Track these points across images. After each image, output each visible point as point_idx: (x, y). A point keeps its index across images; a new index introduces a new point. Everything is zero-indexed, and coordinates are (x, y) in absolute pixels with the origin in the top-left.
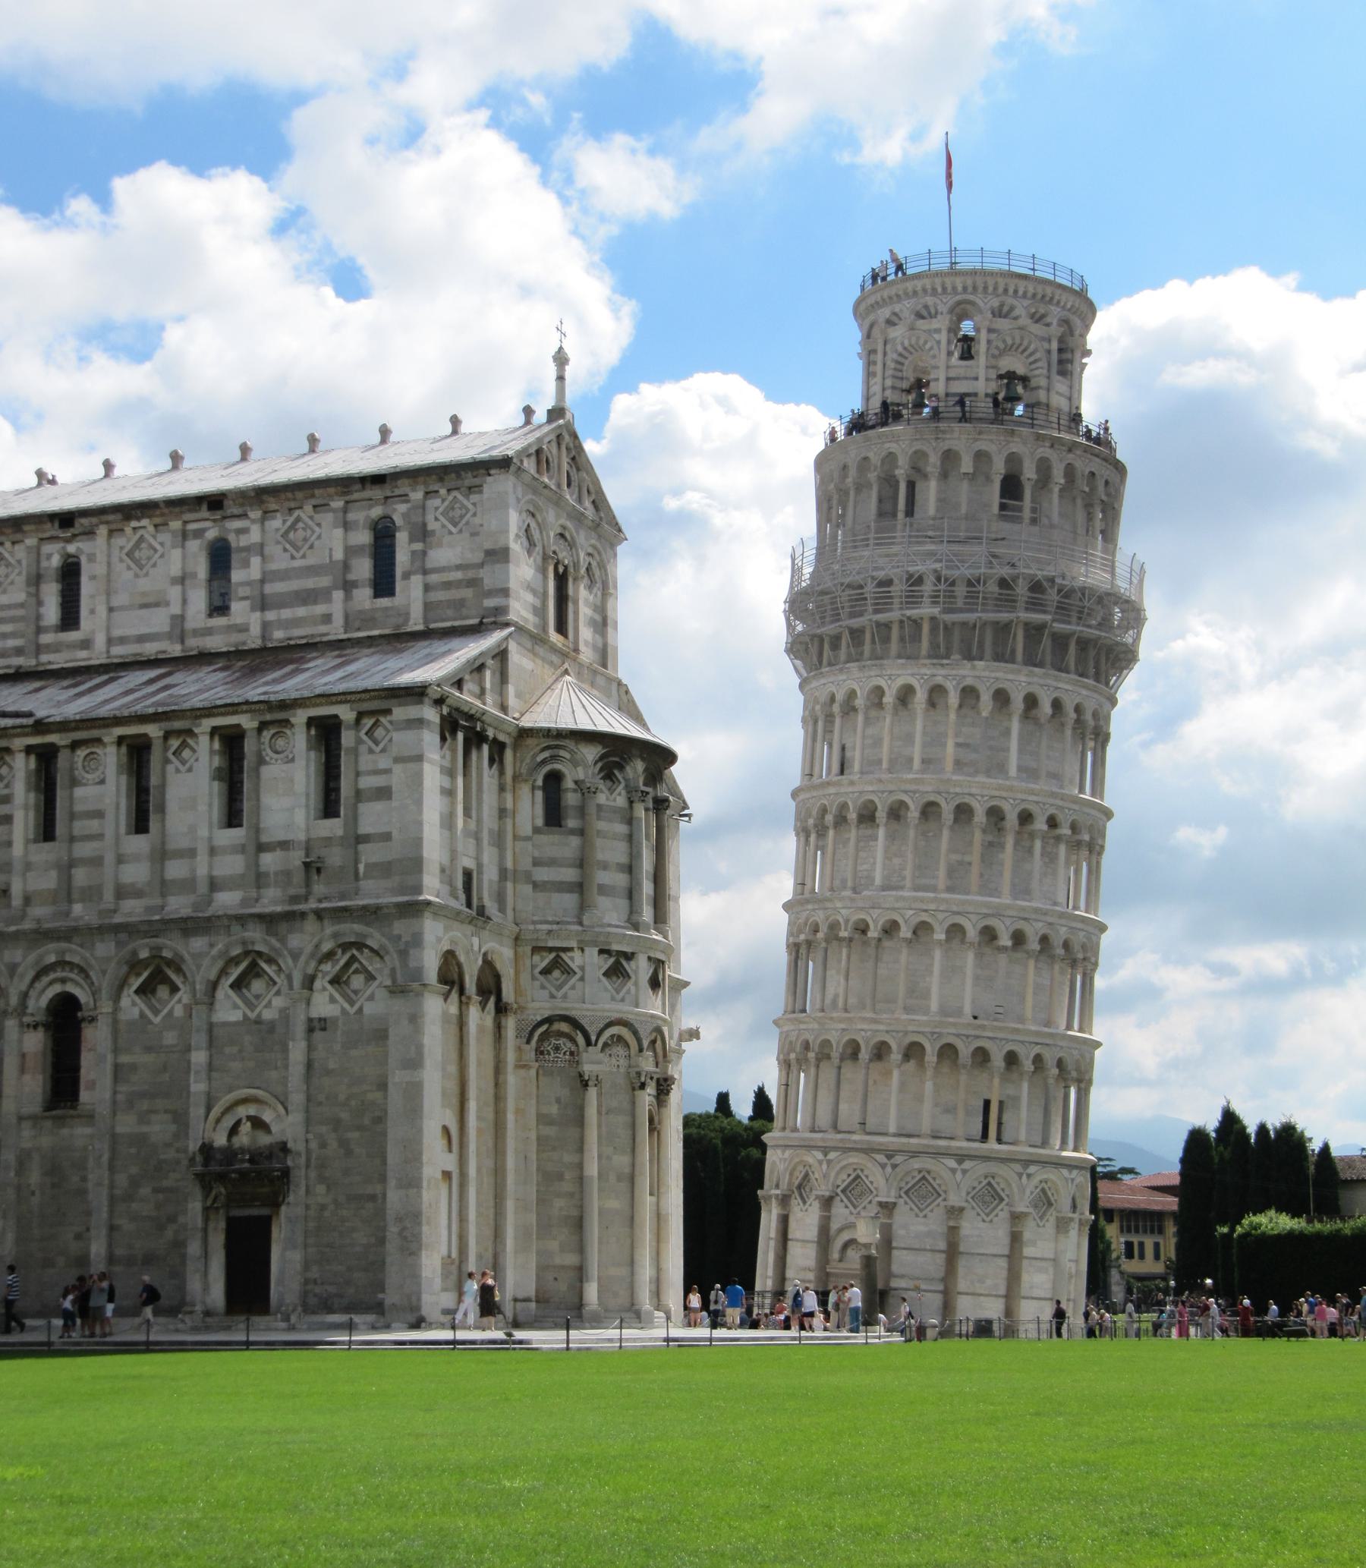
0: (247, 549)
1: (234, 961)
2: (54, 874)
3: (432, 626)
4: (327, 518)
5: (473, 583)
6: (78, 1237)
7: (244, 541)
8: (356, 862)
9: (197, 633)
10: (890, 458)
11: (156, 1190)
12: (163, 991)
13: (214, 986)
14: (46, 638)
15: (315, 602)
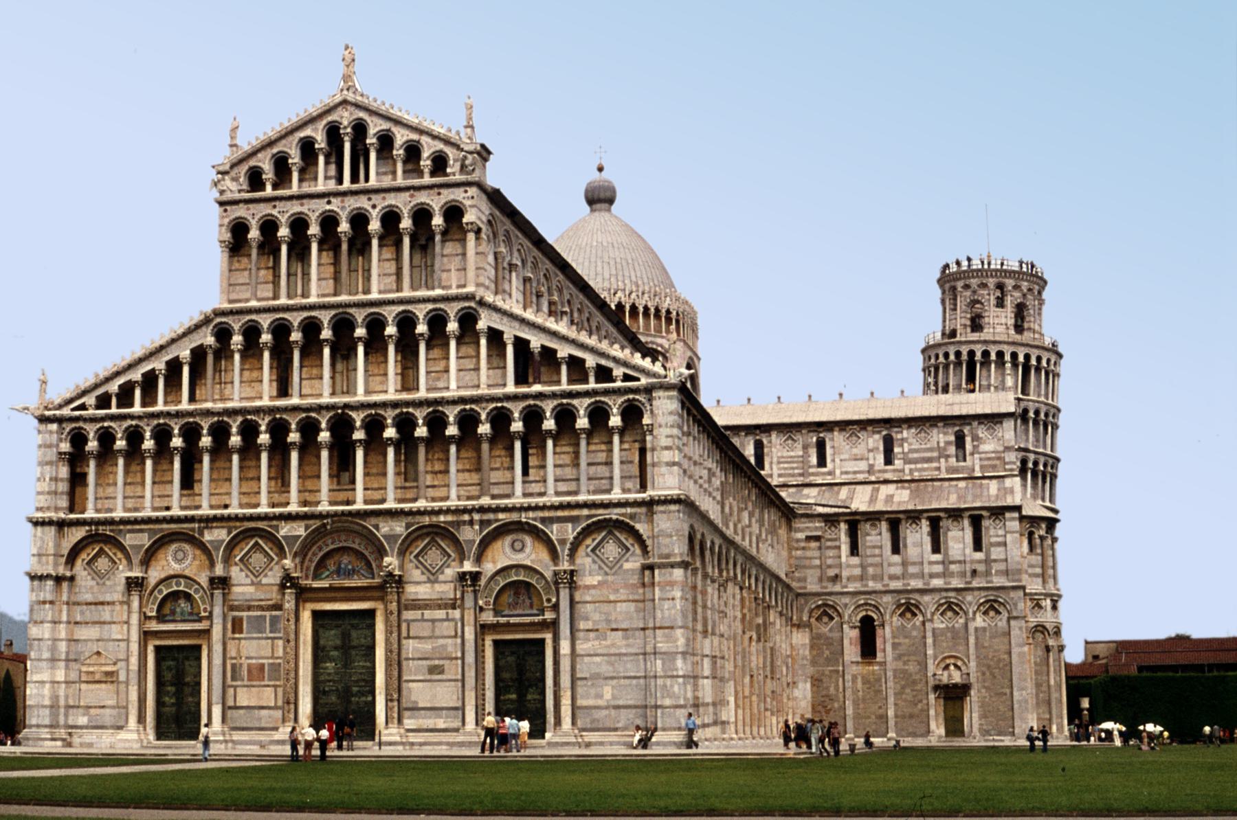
0: (902, 439)
1: (942, 605)
2: (860, 569)
3: (986, 474)
4: (935, 431)
5: (999, 458)
6: (880, 708)
7: (899, 436)
8: (991, 568)
9: (880, 471)
10: (972, 354)
11: (912, 690)
12: (908, 615)
13: (933, 614)
14: (811, 470)
15: (931, 462)
